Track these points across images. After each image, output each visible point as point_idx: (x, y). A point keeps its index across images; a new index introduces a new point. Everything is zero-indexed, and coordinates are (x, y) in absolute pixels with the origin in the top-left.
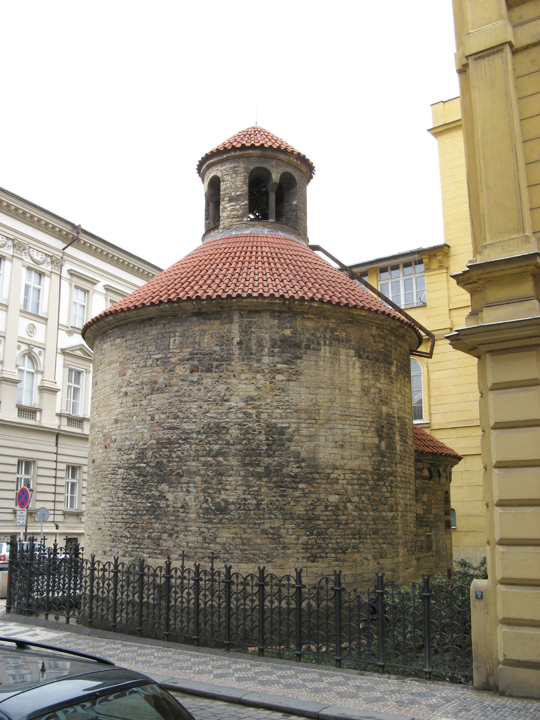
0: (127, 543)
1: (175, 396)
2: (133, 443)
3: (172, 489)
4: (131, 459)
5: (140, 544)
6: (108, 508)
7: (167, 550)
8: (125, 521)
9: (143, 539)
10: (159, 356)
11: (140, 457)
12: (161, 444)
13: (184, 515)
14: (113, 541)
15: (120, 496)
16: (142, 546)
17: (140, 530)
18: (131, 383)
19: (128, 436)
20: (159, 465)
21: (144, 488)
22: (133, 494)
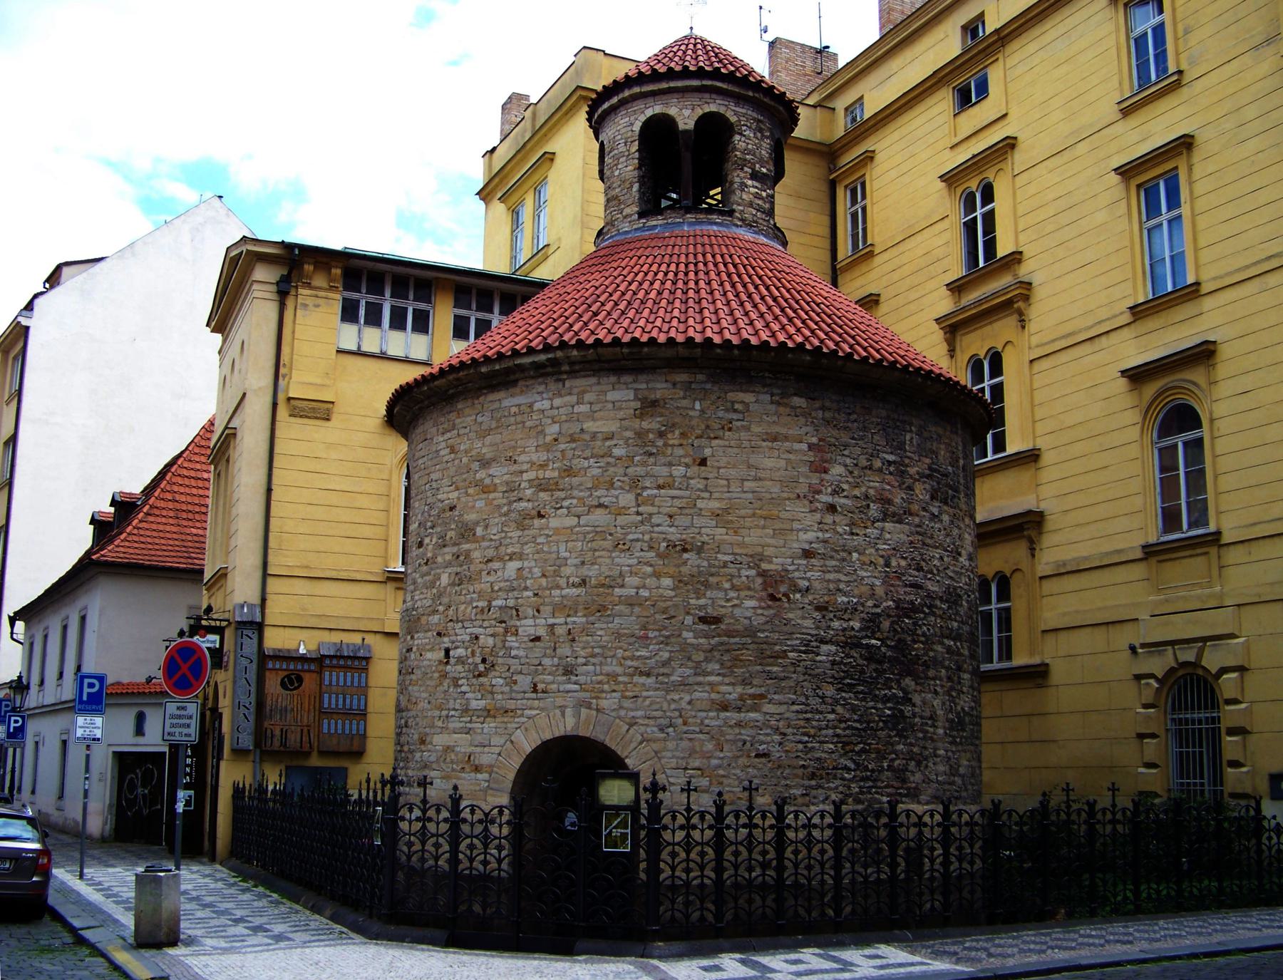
0: (849, 780)
1: (918, 533)
2: (855, 600)
3: (919, 688)
4: (853, 629)
5: (875, 781)
7: (914, 788)
8: (844, 739)
9: (880, 772)
10: (891, 458)
11: (869, 628)
12: (905, 610)
13: (931, 730)
14: (813, 776)
15: (828, 694)
16: (879, 784)
17: (873, 756)
18: (843, 490)
19: (842, 586)
20: (901, 647)
21: (878, 683)
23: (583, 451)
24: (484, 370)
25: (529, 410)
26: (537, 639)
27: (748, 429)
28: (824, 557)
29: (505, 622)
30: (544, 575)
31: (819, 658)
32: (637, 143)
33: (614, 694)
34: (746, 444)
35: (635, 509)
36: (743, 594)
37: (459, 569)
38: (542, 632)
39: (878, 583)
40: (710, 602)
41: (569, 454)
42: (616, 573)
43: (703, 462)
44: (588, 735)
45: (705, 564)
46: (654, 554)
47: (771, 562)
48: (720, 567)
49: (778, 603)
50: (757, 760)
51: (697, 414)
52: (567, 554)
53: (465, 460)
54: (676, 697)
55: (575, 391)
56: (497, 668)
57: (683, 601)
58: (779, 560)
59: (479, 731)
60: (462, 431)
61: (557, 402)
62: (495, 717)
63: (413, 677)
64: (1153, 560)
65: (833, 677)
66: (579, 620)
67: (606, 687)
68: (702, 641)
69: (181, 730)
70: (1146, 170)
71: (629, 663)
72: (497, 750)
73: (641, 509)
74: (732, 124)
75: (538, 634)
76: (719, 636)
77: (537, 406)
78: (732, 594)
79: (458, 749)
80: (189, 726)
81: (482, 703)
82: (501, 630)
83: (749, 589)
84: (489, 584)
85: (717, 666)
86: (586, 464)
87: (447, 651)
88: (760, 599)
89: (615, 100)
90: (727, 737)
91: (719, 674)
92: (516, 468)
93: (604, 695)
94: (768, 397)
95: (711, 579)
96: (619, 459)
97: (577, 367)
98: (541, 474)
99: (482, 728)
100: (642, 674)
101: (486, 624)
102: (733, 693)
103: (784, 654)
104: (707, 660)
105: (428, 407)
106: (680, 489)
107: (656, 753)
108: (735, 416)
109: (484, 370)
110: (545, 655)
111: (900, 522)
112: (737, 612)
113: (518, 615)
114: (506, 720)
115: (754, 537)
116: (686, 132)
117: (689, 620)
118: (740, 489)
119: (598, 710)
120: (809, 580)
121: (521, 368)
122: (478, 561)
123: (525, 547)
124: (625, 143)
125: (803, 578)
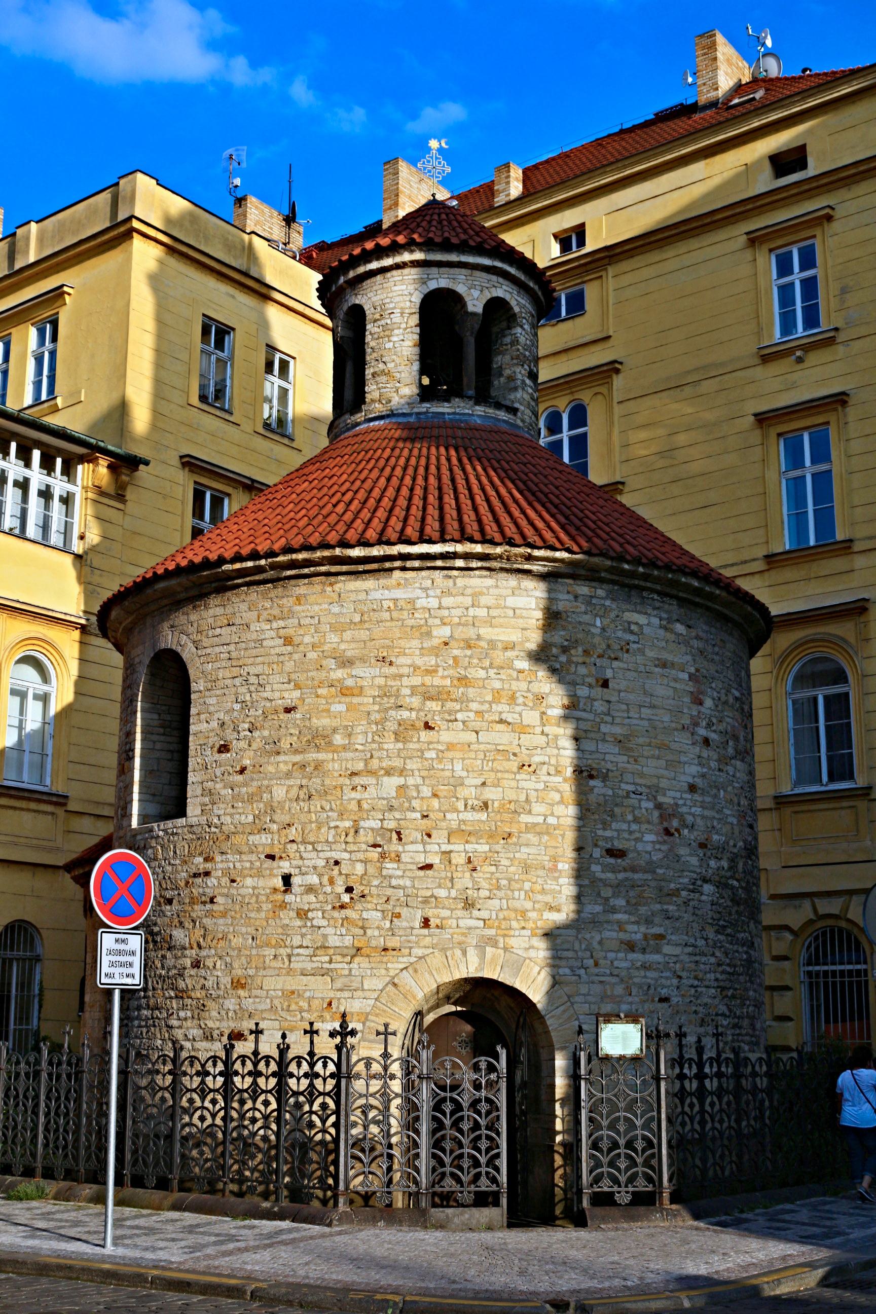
6: (686, 958)
8: (722, 984)
10: (737, 694)
19: (715, 823)
22: (727, 935)
23: (480, 659)
24: (356, 552)
25: (409, 607)
26: (429, 867)
27: (641, 651)
28: (704, 792)
29: (380, 846)
30: (435, 795)
31: (704, 898)
32: (417, 316)
33: (524, 932)
34: (642, 668)
35: (538, 730)
36: (644, 827)
37: (304, 782)
38: (435, 860)
39: (735, 821)
40: (615, 834)
42: (523, 798)
43: (605, 684)
44: (495, 977)
45: (610, 792)
46: (560, 779)
47: (664, 795)
48: (623, 797)
49: (672, 838)
50: (660, 1005)
51: (597, 631)
52: (464, 774)
53: (312, 655)
54: (588, 936)
55: (469, 591)
56: (369, 898)
57: (591, 832)
58: (672, 793)
59: (346, 972)
60: (308, 621)
61: (447, 601)
62: (368, 956)
63: (215, 907)
64: (788, 811)
65: (712, 918)
67: (514, 924)
68: (610, 875)
69: (122, 970)
70: (792, 420)
71: (539, 897)
73: (547, 729)
74: (515, 315)
75: (428, 861)
76: (625, 870)
77: (420, 603)
78: (634, 827)
79: (307, 994)
80: (131, 965)
81: (348, 941)
82: (376, 856)
83: (649, 822)
84: (354, 803)
85: (622, 902)
86: (482, 674)
88: (656, 834)
89: (388, 262)
90: (636, 980)
91: (625, 912)
92: (393, 670)
93: (512, 933)
94: (655, 621)
95: (616, 809)
96: (520, 671)
97: (474, 564)
98: (428, 680)
99: (350, 970)
100: (551, 908)
101: (351, 847)
102: (636, 932)
103: (676, 893)
104: (613, 896)
105: (238, 586)
106: (585, 710)
107: (569, 997)
108: (632, 638)
109: (356, 552)
110: (440, 886)
111: (742, 761)
112: (640, 846)
113: (400, 839)
114: (385, 959)
115: (652, 767)
116: (474, 314)
117: (597, 853)
118: (637, 716)
120: (694, 815)
122: (336, 774)
123: (408, 761)
124: (402, 313)
125: (690, 814)
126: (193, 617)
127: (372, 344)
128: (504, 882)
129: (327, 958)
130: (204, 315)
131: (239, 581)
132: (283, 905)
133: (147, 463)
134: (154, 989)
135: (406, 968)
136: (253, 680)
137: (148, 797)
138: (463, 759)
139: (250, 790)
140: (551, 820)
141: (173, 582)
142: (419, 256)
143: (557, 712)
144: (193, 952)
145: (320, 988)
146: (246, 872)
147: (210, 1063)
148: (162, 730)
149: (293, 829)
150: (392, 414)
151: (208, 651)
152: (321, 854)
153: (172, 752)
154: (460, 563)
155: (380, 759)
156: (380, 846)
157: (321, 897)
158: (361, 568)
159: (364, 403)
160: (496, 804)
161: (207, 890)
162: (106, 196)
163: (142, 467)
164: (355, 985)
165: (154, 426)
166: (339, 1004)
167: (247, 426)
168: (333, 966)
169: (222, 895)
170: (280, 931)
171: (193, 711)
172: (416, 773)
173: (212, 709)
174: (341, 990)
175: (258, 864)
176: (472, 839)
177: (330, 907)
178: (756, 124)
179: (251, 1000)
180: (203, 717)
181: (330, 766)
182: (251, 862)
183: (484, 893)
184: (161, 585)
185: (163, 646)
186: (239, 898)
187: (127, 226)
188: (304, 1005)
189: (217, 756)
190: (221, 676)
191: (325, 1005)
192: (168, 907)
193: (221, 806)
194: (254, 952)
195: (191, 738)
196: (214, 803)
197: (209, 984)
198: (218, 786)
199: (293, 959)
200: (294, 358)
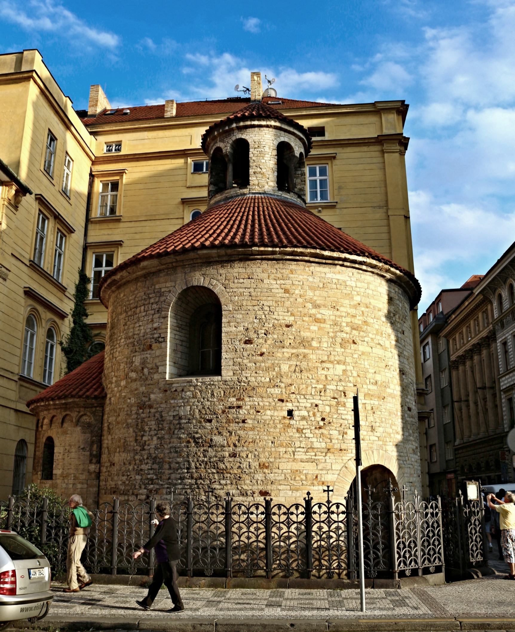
25: (344, 284)
29: (336, 398)
30: (359, 376)
35: (389, 350)
37: (298, 363)
41: (366, 314)
51: (400, 308)
52: (368, 367)
53: (300, 300)
55: (366, 281)
56: (332, 424)
61: (359, 284)
62: (333, 453)
63: (246, 425)
66: (376, 403)
71: (393, 427)
72: (338, 472)
79: (304, 472)
81: (323, 445)
82: (335, 403)
84: (324, 376)
87: (290, 413)
89: (263, 123)
92: (338, 313)
97: (369, 269)
99: (326, 460)
101: (323, 398)
113: (345, 396)
114: (341, 455)
116: (296, 157)
119: (386, 451)
121: (345, 260)
122: (314, 361)
124: (269, 148)
126: (222, 271)
127: (254, 158)
128: (384, 420)
129: (314, 454)
130: (49, 130)
131: (259, 257)
132: (289, 426)
133: (31, 193)
134: (196, 468)
135: (350, 459)
136: (266, 308)
137: (172, 364)
138: (368, 360)
139: (267, 365)
140: (395, 392)
141: (214, 251)
142: (278, 124)
143: (394, 343)
144: (231, 448)
145: (310, 469)
146: (267, 407)
147: (294, 507)
148: (178, 329)
149: (293, 387)
150: (264, 193)
151: (235, 290)
152: (308, 401)
153: (182, 341)
154: (364, 267)
155: (334, 356)
156: (336, 398)
157: (309, 422)
158: (324, 261)
159: (249, 185)
160: (379, 383)
161: (241, 416)
162: (13, 57)
163: (28, 194)
164: (329, 467)
165: (28, 176)
166: (321, 477)
167: (57, 187)
168: (317, 457)
169: (251, 419)
170: (288, 439)
171: (224, 320)
172: (350, 364)
173: (239, 320)
174: (322, 470)
175: (274, 403)
176: (372, 398)
177: (314, 428)
178: (304, 113)
179: (272, 475)
180: (231, 324)
181: (311, 356)
182: (269, 402)
183: (378, 424)
184: (205, 252)
185: (195, 284)
186: (263, 421)
187: (30, 74)
188: (304, 477)
189: (244, 346)
190: (245, 304)
191: (314, 478)
192: (208, 424)
193: (248, 372)
194: (273, 449)
195: (223, 335)
196: (242, 370)
197: (244, 465)
198: (245, 361)
199: (296, 453)
200: (73, 161)
